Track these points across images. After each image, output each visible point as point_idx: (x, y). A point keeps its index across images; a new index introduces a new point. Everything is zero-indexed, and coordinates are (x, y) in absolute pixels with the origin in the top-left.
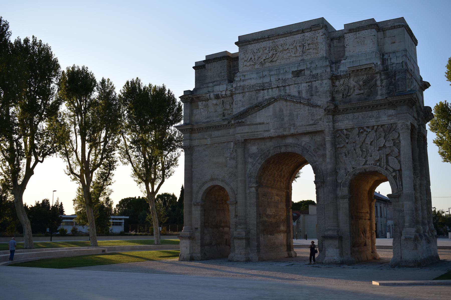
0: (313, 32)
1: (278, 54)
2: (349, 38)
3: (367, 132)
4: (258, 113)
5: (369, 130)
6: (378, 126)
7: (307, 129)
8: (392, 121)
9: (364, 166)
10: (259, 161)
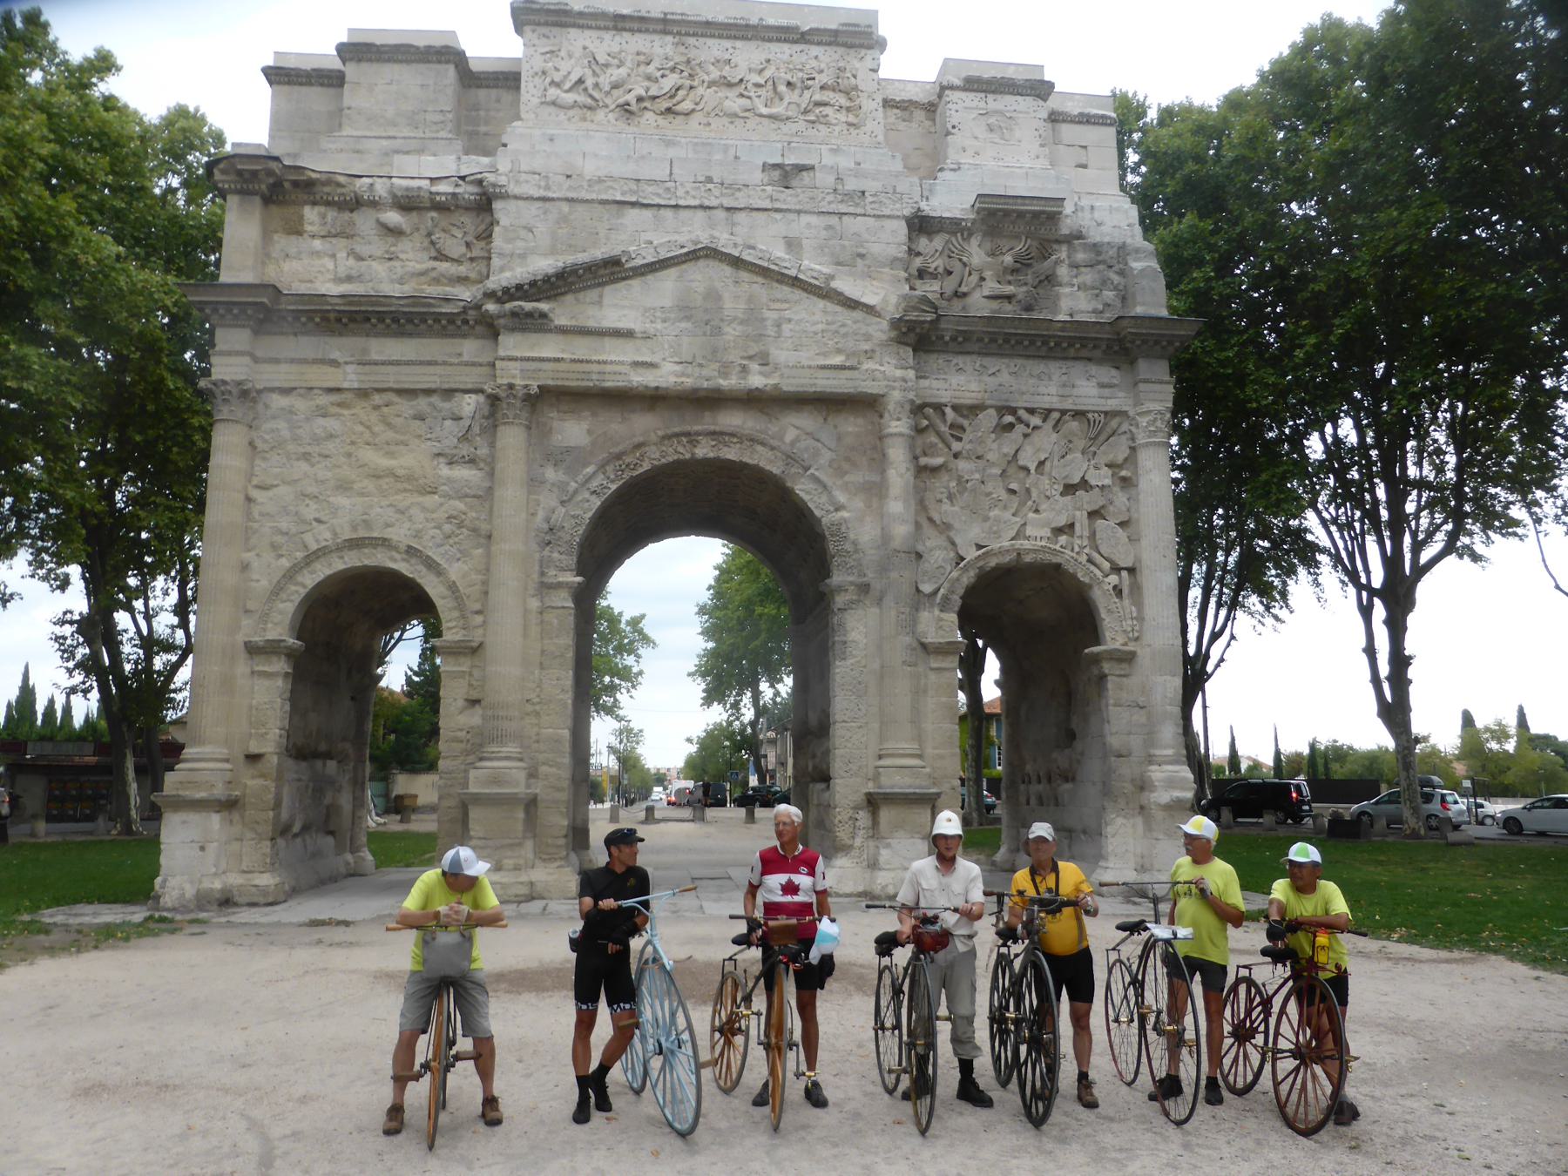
0: (841, 50)
1: (700, 91)
2: (961, 108)
3: (1028, 426)
4: (608, 289)
5: (1035, 420)
6: (1063, 412)
7: (820, 382)
8: (1112, 404)
9: (1018, 543)
10: (594, 484)
